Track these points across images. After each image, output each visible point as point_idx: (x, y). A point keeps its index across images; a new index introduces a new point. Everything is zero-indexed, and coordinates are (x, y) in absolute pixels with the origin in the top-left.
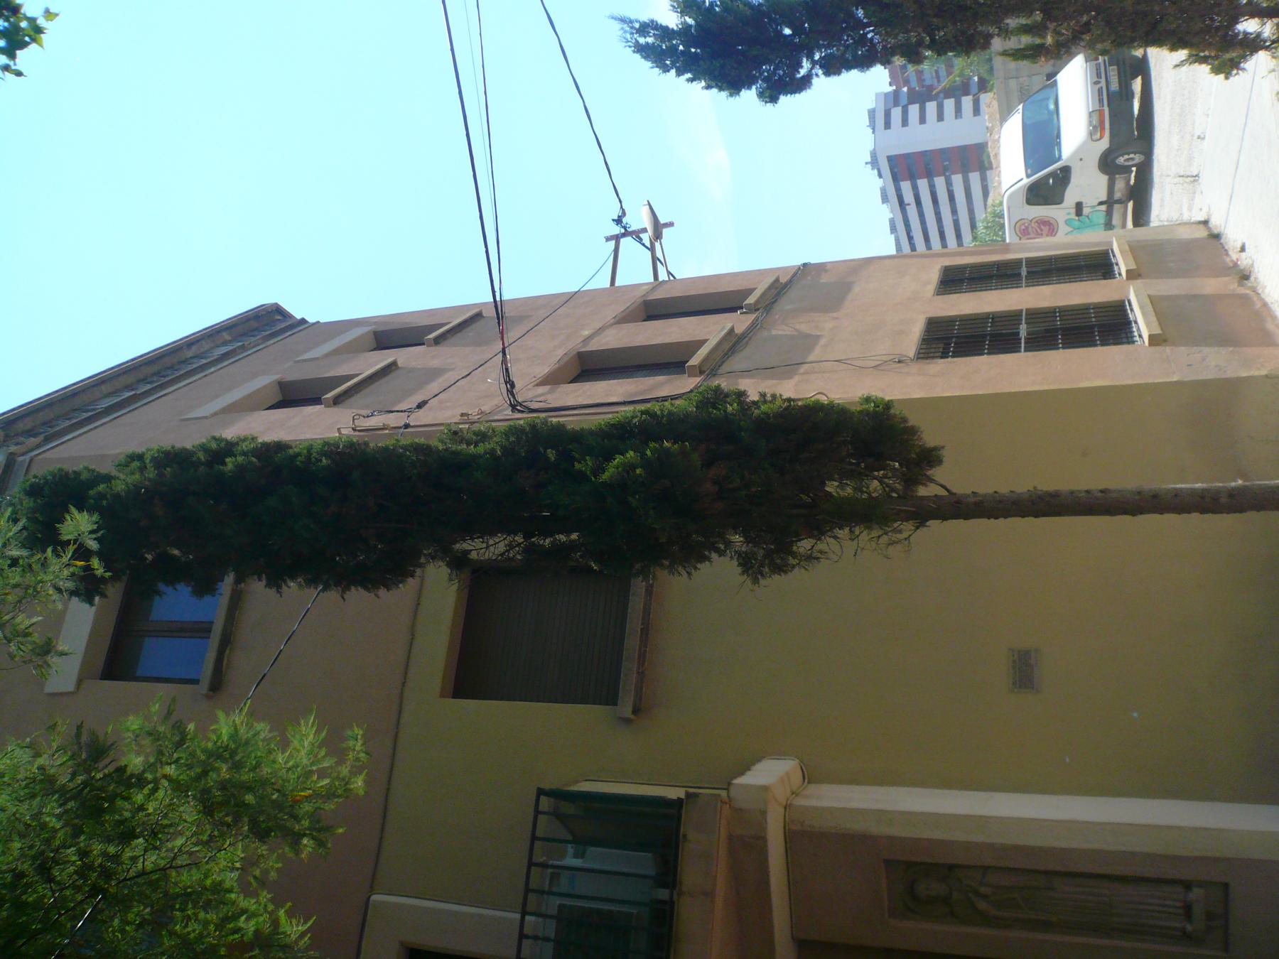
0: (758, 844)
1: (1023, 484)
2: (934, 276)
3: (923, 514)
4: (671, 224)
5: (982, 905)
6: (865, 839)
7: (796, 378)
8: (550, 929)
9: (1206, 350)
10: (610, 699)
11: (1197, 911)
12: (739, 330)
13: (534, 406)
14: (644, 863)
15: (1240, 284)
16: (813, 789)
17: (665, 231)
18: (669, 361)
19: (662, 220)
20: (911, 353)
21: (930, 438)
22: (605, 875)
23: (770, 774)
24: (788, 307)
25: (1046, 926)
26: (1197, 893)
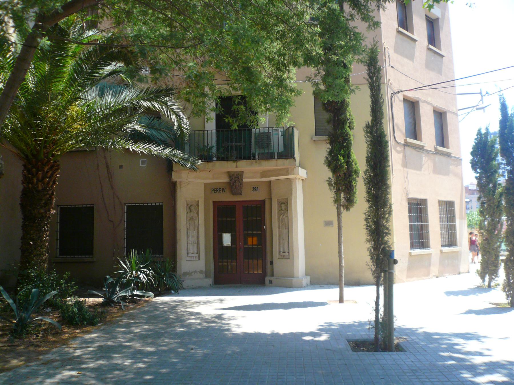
0: (287, 173)
1: (343, 224)
2: (449, 199)
3: (338, 208)
4: (484, 111)
5: (281, 216)
6: (291, 194)
7: (402, 168)
8: (266, 131)
9: (407, 264)
10: (317, 134)
11: (284, 254)
12: (425, 148)
13: (393, 99)
14: (281, 149)
15: (434, 276)
16: (301, 182)
17: (482, 110)
18: (414, 130)
19: (485, 109)
20: (411, 196)
21: (351, 209)
22: (278, 143)
23: (302, 173)
24: (437, 159)
25: (279, 228)
26: (287, 254)
